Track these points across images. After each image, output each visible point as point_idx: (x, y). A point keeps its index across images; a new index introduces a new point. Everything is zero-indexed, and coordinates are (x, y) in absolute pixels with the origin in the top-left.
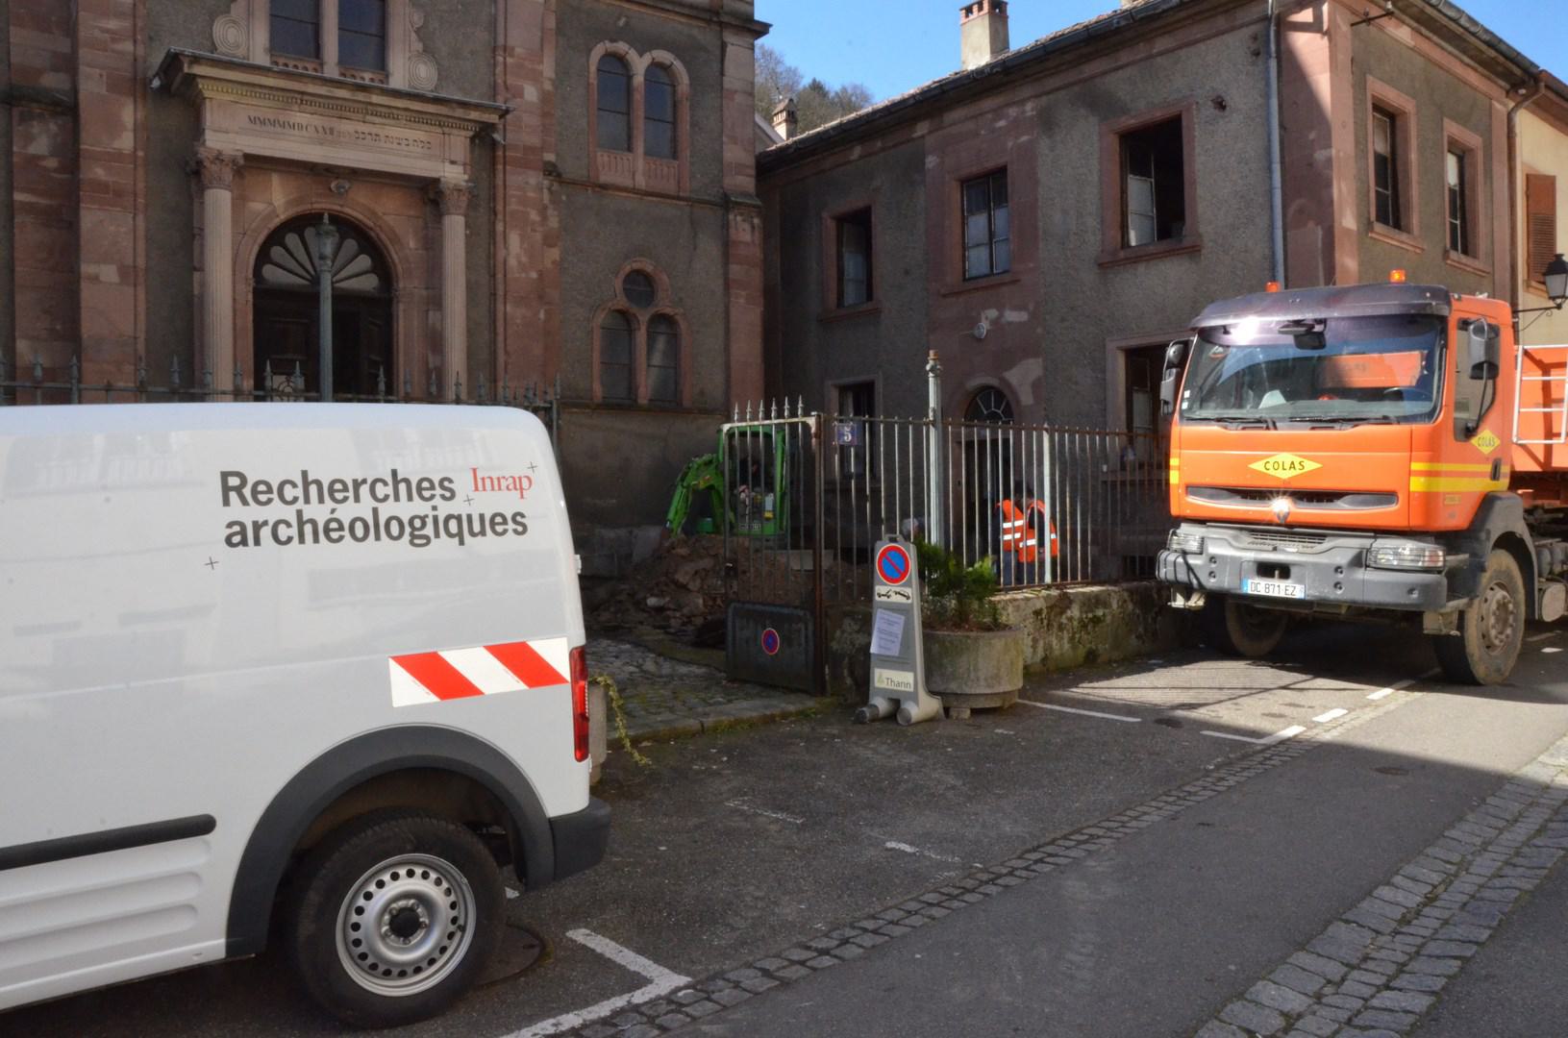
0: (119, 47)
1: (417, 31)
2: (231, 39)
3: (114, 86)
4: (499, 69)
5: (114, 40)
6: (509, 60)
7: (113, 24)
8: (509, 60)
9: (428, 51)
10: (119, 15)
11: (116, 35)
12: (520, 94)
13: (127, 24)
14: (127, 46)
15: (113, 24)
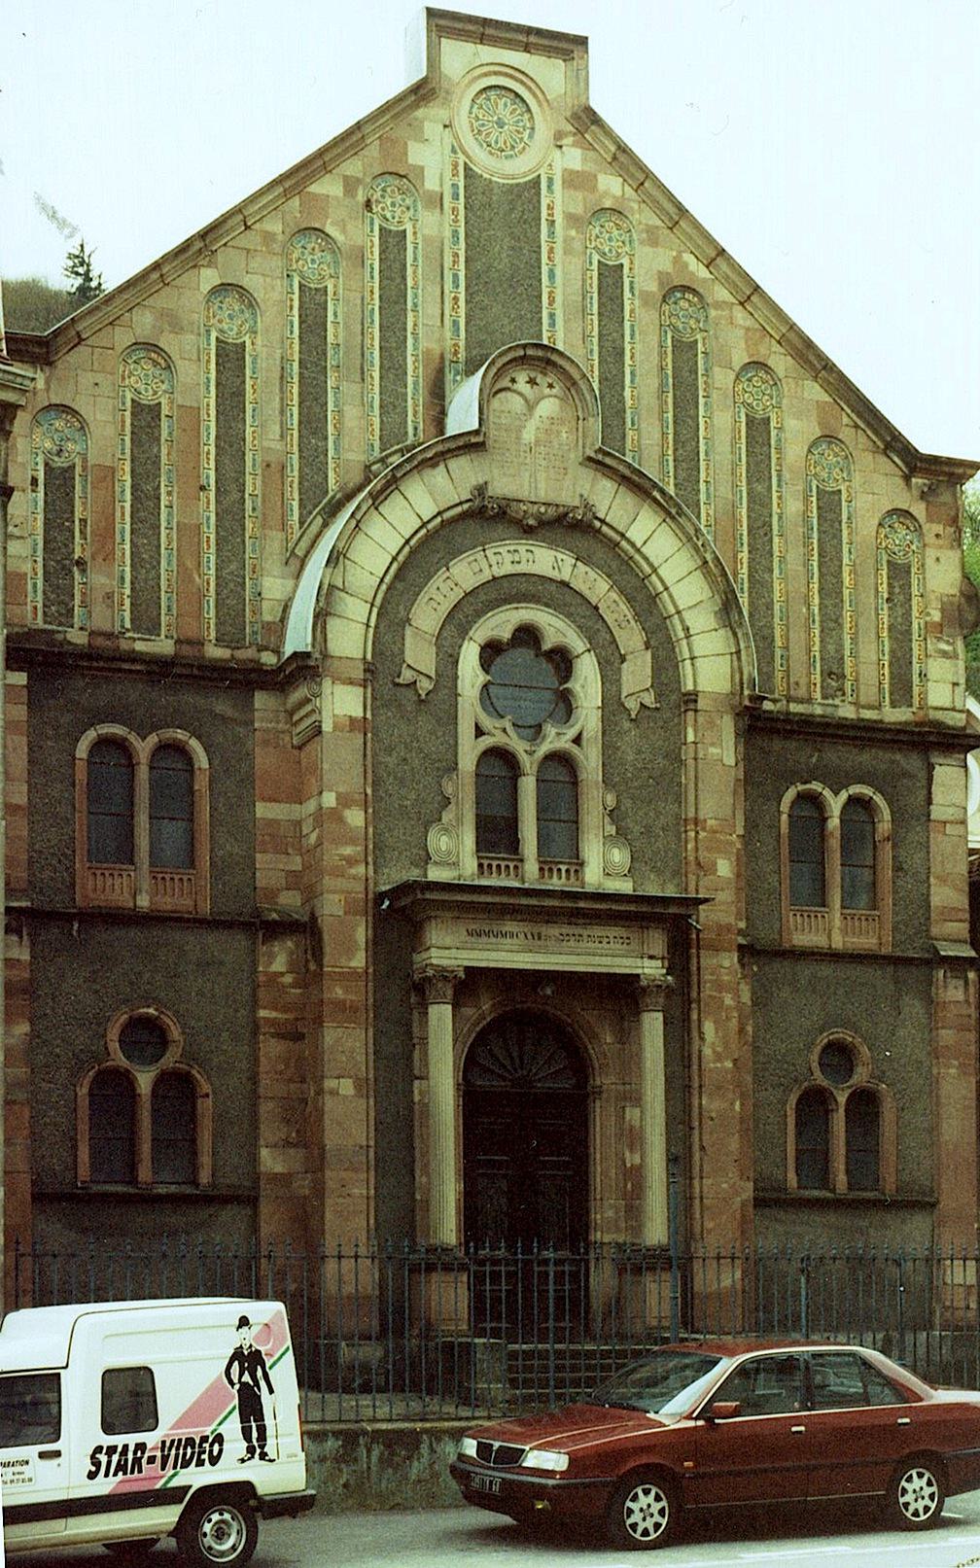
0: (353, 871)
6: (702, 834)
7: (348, 851)
9: (622, 835)
10: (353, 841)
11: (351, 861)
12: (712, 869)
14: (361, 869)
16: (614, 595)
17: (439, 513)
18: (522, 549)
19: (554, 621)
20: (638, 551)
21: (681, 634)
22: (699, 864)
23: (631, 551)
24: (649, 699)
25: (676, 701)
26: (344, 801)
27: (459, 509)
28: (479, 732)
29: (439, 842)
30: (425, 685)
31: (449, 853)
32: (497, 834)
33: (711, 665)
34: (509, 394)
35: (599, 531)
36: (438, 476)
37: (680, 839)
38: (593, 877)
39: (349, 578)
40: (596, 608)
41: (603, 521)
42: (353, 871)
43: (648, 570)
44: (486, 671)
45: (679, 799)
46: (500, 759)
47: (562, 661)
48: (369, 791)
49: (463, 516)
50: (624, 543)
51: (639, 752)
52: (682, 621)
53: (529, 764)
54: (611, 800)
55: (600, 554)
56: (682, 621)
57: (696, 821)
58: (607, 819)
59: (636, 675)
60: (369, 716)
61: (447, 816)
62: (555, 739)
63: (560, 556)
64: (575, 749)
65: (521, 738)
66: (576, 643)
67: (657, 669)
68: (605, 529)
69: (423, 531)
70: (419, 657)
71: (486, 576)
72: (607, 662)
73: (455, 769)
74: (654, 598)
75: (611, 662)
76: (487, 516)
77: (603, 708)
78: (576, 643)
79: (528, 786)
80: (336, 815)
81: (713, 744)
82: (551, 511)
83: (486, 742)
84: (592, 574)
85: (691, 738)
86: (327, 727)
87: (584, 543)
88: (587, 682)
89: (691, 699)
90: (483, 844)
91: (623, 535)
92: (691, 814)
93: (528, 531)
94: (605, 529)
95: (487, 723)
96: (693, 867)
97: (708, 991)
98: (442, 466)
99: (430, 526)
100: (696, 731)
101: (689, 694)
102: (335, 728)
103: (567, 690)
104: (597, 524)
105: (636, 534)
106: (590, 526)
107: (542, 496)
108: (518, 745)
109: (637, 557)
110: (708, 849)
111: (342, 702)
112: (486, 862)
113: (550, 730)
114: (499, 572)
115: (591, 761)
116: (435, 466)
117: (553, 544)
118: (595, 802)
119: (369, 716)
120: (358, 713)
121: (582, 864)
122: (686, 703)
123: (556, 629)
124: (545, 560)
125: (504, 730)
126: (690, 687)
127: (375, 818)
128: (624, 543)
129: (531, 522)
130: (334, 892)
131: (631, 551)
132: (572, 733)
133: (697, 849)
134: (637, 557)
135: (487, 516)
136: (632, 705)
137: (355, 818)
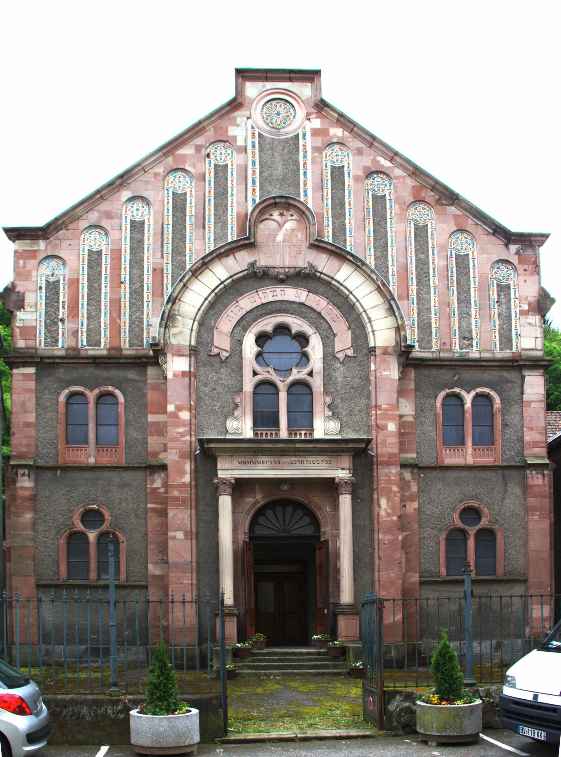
0: (183, 439)
1: (329, 406)
2: (235, 426)
3: (182, 456)
4: (373, 418)
5: (182, 436)
6: (378, 412)
7: (181, 430)
8: (378, 412)
9: (335, 416)
10: (184, 425)
11: (182, 435)
12: (386, 427)
13: (187, 428)
14: (188, 438)
15: (181, 430)
16: (331, 307)
17: (231, 277)
18: (278, 290)
19: (296, 321)
20: (341, 284)
21: (367, 321)
22: (377, 426)
23: (338, 285)
24: (350, 353)
25: (364, 350)
26: (179, 408)
27: (242, 274)
28: (255, 374)
29: (232, 424)
30: (225, 354)
31: (238, 429)
32: (265, 418)
33: (382, 334)
34: (269, 222)
35: (320, 277)
36: (230, 261)
37: (369, 416)
38: (318, 434)
39: (181, 309)
40: (320, 313)
41: (321, 273)
42: (183, 439)
43: (348, 293)
44: (258, 346)
45: (368, 397)
46: (265, 387)
47: (302, 339)
48: (192, 403)
49: (244, 278)
50: (333, 282)
51: (345, 377)
52: (367, 315)
53: (282, 387)
54: (328, 400)
55: (322, 288)
56: (367, 315)
57: (376, 406)
58: (327, 409)
59: (344, 341)
60: (192, 370)
61: (236, 413)
62: (296, 374)
63: (299, 291)
64: (309, 378)
65: (277, 374)
66: (308, 329)
67: (354, 340)
68: (322, 276)
69: (222, 286)
70: (222, 342)
71: (259, 303)
72: (327, 337)
73: (242, 391)
74: (352, 307)
75: (328, 339)
76: (258, 277)
77: (324, 359)
78: (308, 329)
79: (283, 396)
80: (175, 415)
81: (385, 370)
82: (292, 270)
83: (258, 378)
84: (317, 298)
85: (373, 367)
86: (170, 376)
87: (312, 285)
88: (316, 349)
89: (372, 350)
90: (256, 424)
91: (333, 278)
92: (373, 403)
93: (282, 282)
94: (322, 276)
95: (258, 369)
96: (374, 428)
97: (382, 485)
98: (231, 257)
99: (226, 283)
100: (375, 364)
101: (371, 348)
102: (175, 375)
103: (305, 351)
104: (318, 274)
105: (340, 277)
106: (316, 276)
107: (287, 264)
108: (275, 378)
109: (341, 288)
110: (383, 419)
111: (176, 365)
112: (259, 432)
113: (295, 371)
114: (264, 301)
115: (317, 383)
116: (228, 256)
117: (295, 286)
118: (320, 402)
119: (192, 370)
120: (187, 369)
121: (313, 431)
122: (370, 352)
123: (297, 324)
124: (291, 294)
125: (268, 372)
126: (372, 344)
127: (194, 416)
128: (333, 282)
129: (282, 277)
130: (172, 449)
131: (338, 285)
132: (307, 370)
133: (376, 419)
134: (341, 288)
135: (258, 277)
136: (341, 356)
137: (185, 415)
